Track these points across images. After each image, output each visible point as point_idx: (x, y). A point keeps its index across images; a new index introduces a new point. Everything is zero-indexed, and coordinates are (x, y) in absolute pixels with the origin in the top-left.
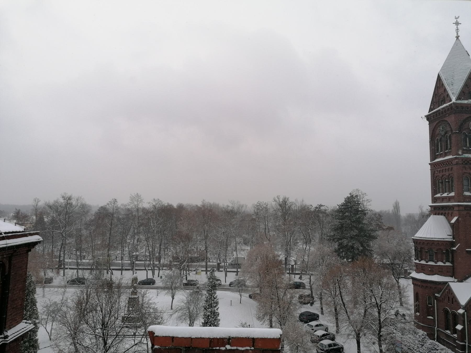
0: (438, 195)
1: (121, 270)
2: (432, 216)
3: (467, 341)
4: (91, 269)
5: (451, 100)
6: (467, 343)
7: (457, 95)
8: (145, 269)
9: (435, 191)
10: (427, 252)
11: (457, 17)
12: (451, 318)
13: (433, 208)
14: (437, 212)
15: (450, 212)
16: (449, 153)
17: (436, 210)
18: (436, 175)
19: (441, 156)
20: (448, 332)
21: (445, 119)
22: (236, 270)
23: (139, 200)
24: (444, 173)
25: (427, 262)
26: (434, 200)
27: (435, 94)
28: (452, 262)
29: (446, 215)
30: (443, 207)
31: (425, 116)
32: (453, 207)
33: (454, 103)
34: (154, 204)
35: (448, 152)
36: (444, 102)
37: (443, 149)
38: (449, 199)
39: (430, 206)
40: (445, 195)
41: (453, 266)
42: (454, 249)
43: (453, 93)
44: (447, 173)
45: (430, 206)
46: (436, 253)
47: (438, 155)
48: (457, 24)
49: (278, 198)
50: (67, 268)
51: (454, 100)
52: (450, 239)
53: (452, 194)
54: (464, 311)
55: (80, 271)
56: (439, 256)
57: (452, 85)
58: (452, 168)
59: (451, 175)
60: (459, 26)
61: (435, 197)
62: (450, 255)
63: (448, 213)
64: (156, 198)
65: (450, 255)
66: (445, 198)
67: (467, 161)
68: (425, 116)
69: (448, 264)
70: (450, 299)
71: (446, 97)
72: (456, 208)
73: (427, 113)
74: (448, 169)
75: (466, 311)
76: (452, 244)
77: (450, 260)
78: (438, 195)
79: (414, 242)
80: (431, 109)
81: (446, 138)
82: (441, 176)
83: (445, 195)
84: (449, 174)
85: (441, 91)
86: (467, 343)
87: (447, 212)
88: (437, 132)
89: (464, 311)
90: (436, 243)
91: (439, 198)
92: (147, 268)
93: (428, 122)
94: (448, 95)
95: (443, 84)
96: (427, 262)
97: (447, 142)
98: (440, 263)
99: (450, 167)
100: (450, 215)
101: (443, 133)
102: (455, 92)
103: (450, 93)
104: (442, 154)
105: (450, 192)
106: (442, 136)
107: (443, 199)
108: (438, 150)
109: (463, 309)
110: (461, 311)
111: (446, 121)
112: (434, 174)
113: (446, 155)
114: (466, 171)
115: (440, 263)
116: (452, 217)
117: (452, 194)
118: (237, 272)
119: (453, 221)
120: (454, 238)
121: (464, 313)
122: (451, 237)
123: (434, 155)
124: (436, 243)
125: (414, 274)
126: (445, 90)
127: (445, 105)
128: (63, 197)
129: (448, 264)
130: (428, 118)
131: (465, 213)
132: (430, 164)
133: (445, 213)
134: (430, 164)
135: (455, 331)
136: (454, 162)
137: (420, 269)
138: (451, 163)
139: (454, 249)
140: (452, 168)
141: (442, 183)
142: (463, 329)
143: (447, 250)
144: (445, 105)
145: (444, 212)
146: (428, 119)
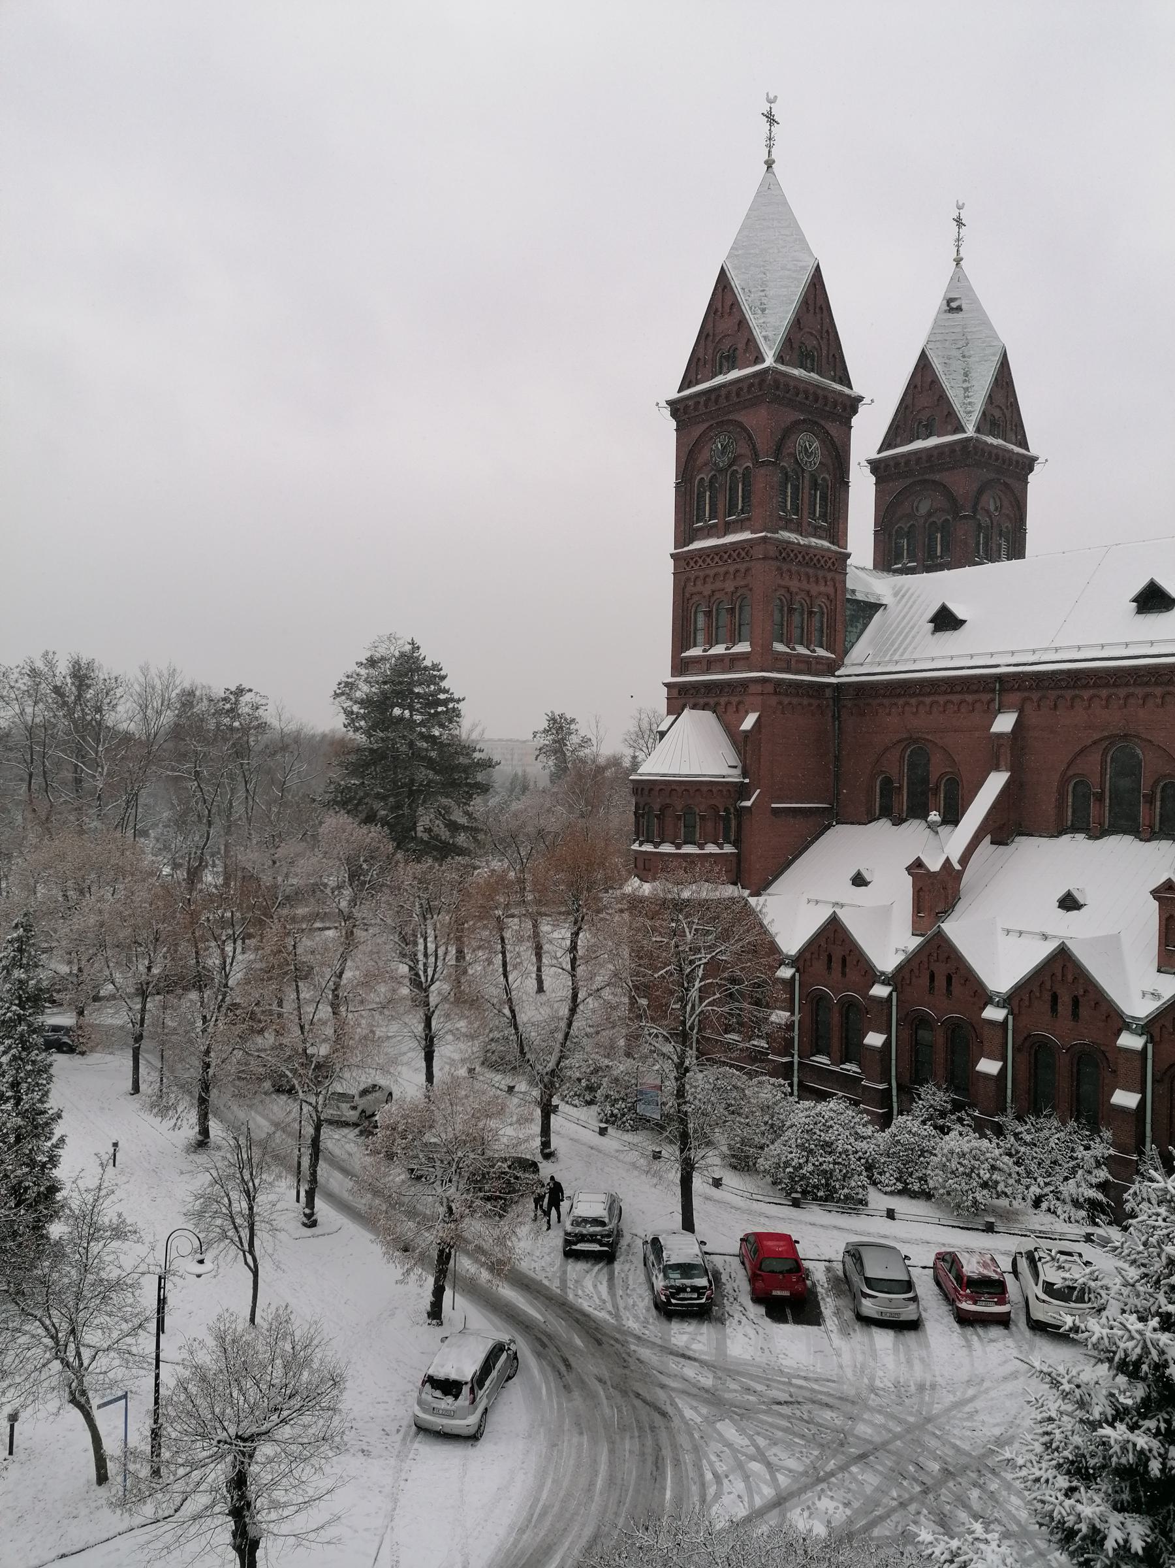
2: (686, 711)
3: (796, 1052)
5: (759, 359)
6: (796, 1056)
7: (776, 346)
9: (683, 636)
10: (679, 818)
11: (771, 96)
13: (675, 692)
14: (702, 701)
16: (740, 526)
18: (690, 588)
19: (710, 532)
24: (718, 585)
25: (678, 847)
26: (680, 665)
27: (705, 335)
28: (736, 843)
29: (721, 709)
30: (709, 687)
31: (668, 402)
32: (744, 684)
33: (766, 371)
35: (734, 522)
36: (732, 361)
38: (733, 662)
39: (666, 685)
40: (719, 649)
41: (738, 855)
42: (748, 804)
43: (765, 338)
44: (730, 586)
45: (666, 685)
46: (702, 818)
48: (771, 119)
51: (769, 361)
52: (734, 776)
53: (743, 647)
54: (793, 970)
56: (710, 825)
57: (763, 310)
58: (747, 570)
60: (775, 128)
61: (683, 659)
62: (733, 823)
63: (728, 703)
65: (733, 823)
66: (719, 658)
67: (786, 552)
68: (668, 402)
69: (729, 849)
71: (741, 346)
72: (753, 688)
73: (674, 395)
74: (697, 578)
75: (797, 971)
76: (742, 791)
80: (686, 383)
82: (707, 593)
83: (719, 649)
85: (726, 325)
86: (796, 1056)
89: (793, 970)
90: (704, 789)
91: (696, 660)
93: (673, 424)
94: (751, 341)
95: (735, 304)
96: (678, 847)
97: (733, 489)
98: (711, 849)
99: (742, 567)
100: (732, 709)
102: (770, 334)
103: (758, 334)
104: (715, 525)
105: (734, 640)
106: (721, 471)
107: (710, 663)
108: (701, 509)
111: (740, 425)
113: (728, 529)
114: (783, 583)
115: (711, 849)
117: (743, 647)
119: (748, 723)
120: (745, 774)
121: (793, 976)
122: (738, 772)
123: (685, 530)
124: (704, 789)
125: (635, 886)
126: (742, 323)
127: (735, 374)
129: (729, 849)
130: (677, 408)
131: (773, 701)
132: (672, 555)
133: (717, 704)
134: (672, 555)
136: (758, 552)
137: (645, 867)
138: (688, 564)
139: (748, 804)
141: (708, 614)
143: (726, 810)
144: (735, 374)
145: (712, 701)
146: (674, 414)
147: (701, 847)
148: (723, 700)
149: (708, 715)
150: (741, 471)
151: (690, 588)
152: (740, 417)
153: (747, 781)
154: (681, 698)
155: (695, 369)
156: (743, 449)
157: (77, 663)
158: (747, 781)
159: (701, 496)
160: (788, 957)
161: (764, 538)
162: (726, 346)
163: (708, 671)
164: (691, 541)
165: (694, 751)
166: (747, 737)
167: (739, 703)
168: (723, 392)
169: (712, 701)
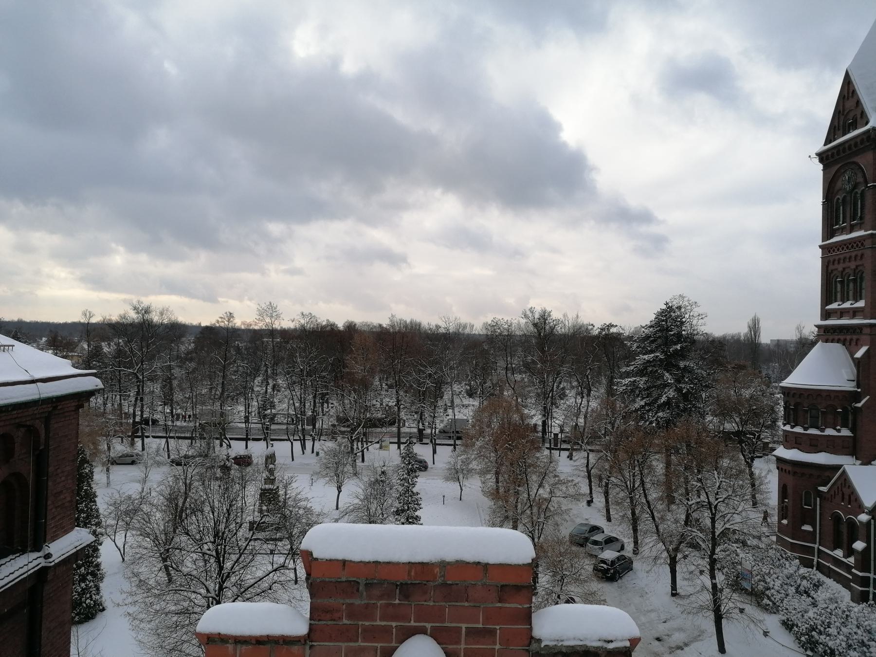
0: (834, 306)
1: (246, 440)
4: (191, 438)
8: (289, 440)
9: (828, 295)
10: (806, 411)
12: (844, 529)
13: (822, 330)
14: (831, 337)
15: (855, 337)
16: (860, 227)
17: (827, 334)
18: (831, 267)
19: (842, 231)
20: (839, 553)
21: (857, 159)
22: (451, 442)
23: (275, 314)
25: (806, 429)
26: (826, 314)
28: (852, 430)
31: (817, 154)
34: (302, 321)
35: (856, 224)
37: (848, 219)
38: (854, 313)
40: (847, 305)
42: (859, 405)
44: (853, 265)
47: (838, 229)
49: (532, 312)
50: (148, 437)
52: (850, 387)
53: (861, 304)
55: (172, 442)
58: (862, 255)
59: (860, 268)
61: (827, 310)
62: (850, 417)
63: (851, 340)
64: (306, 312)
65: (850, 417)
68: (817, 154)
69: (846, 432)
70: (847, 497)
71: (859, 116)
72: (867, 331)
76: (855, 396)
77: (850, 426)
78: (834, 306)
79: (784, 394)
81: (855, 197)
83: (847, 305)
84: (857, 266)
85: (850, 104)
87: (848, 337)
88: (839, 184)
92: (291, 438)
93: (821, 166)
95: (854, 91)
96: (806, 429)
98: (830, 432)
99: (859, 253)
100: (854, 343)
101: (848, 187)
104: (845, 227)
105: (856, 300)
106: (847, 193)
107: (842, 313)
109: (869, 513)
110: (864, 517)
112: (827, 267)
113: (852, 229)
115: (830, 432)
116: (858, 346)
117: (861, 304)
118: (455, 445)
119: (859, 354)
120: (858, 386)
122: (855, 383)
125: (782, 452)
126: (858, 103)
128: (135, 308)
129: (846, 432)
130: (822, 157)
132: (820, 247)
133: (845, 340)
135: (850, 552)
137: (792, 441)
138: (862, 244)
139: (859, 405)
140: (862, 255)
141: (842, 282)
142: (867, 550)
145: (842, 338)
146: (821, 161)
147: (823, 430)
148: (848, 337)
149: (838, 346)
150: (859, 192)
151: (831, 267)
152: (857, 159)
153: (859, 390)
154: (827, 334)
155: (834, 131)
156: (860, 179)
157: (545, 312)
158: (859, 390)
159: (838, 210)
160: (867, 508)
161: (872, 234)
162: (851, 115)
163: (841, 317)
164: (832, 237)
165: (822, 370)
166: (859, 362)
167: (857, 340)
168: (847, 145)
169: (842, 338)
